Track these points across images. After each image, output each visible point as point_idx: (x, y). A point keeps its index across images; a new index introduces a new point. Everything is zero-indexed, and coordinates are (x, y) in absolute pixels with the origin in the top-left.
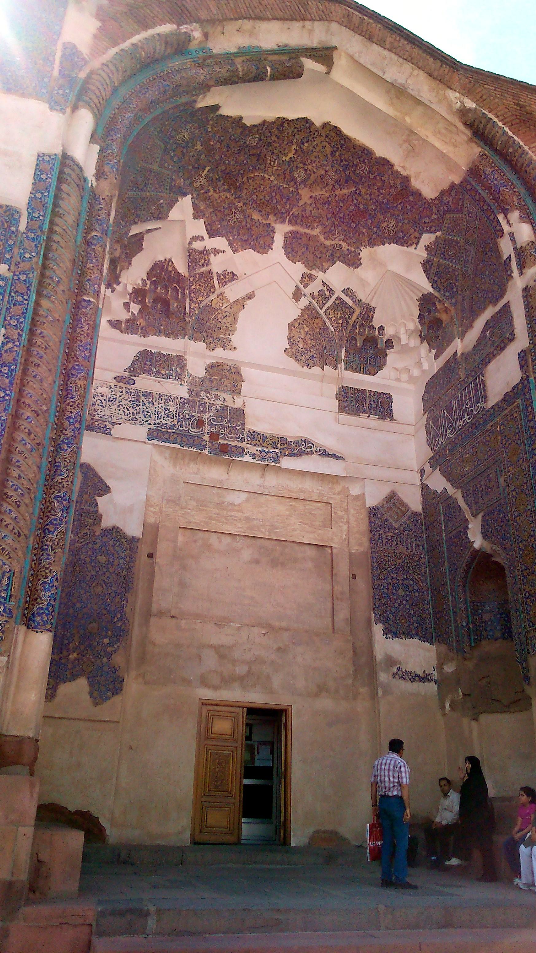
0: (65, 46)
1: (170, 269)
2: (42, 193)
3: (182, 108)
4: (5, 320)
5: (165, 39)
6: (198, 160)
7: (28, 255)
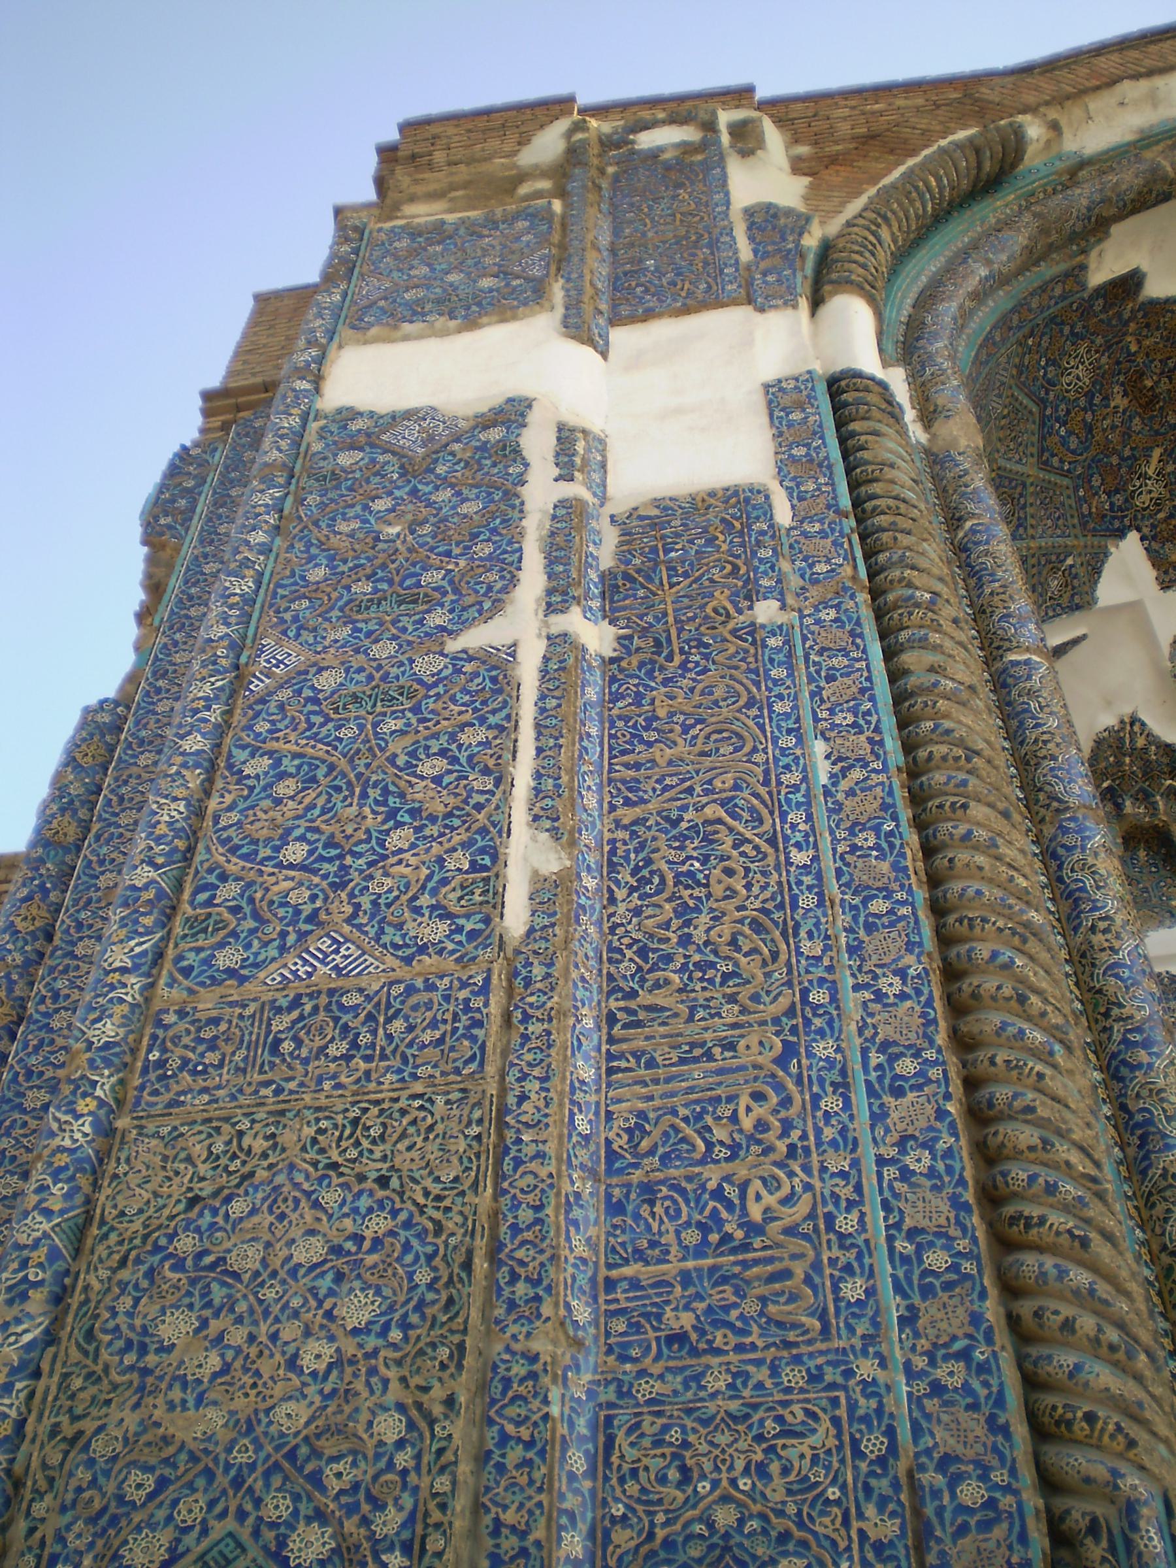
0: (749, 212)
1: (1141, 742)
2: (808, 446)
3: (1058, 291)
4: (816, 720)
5: (974, 147)
6: (1127, 435)
7: (821, 568)
